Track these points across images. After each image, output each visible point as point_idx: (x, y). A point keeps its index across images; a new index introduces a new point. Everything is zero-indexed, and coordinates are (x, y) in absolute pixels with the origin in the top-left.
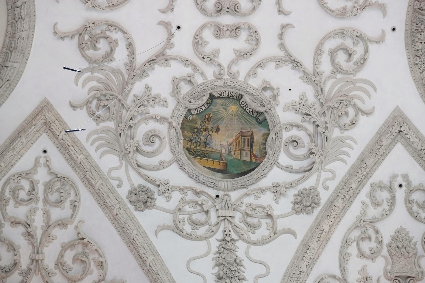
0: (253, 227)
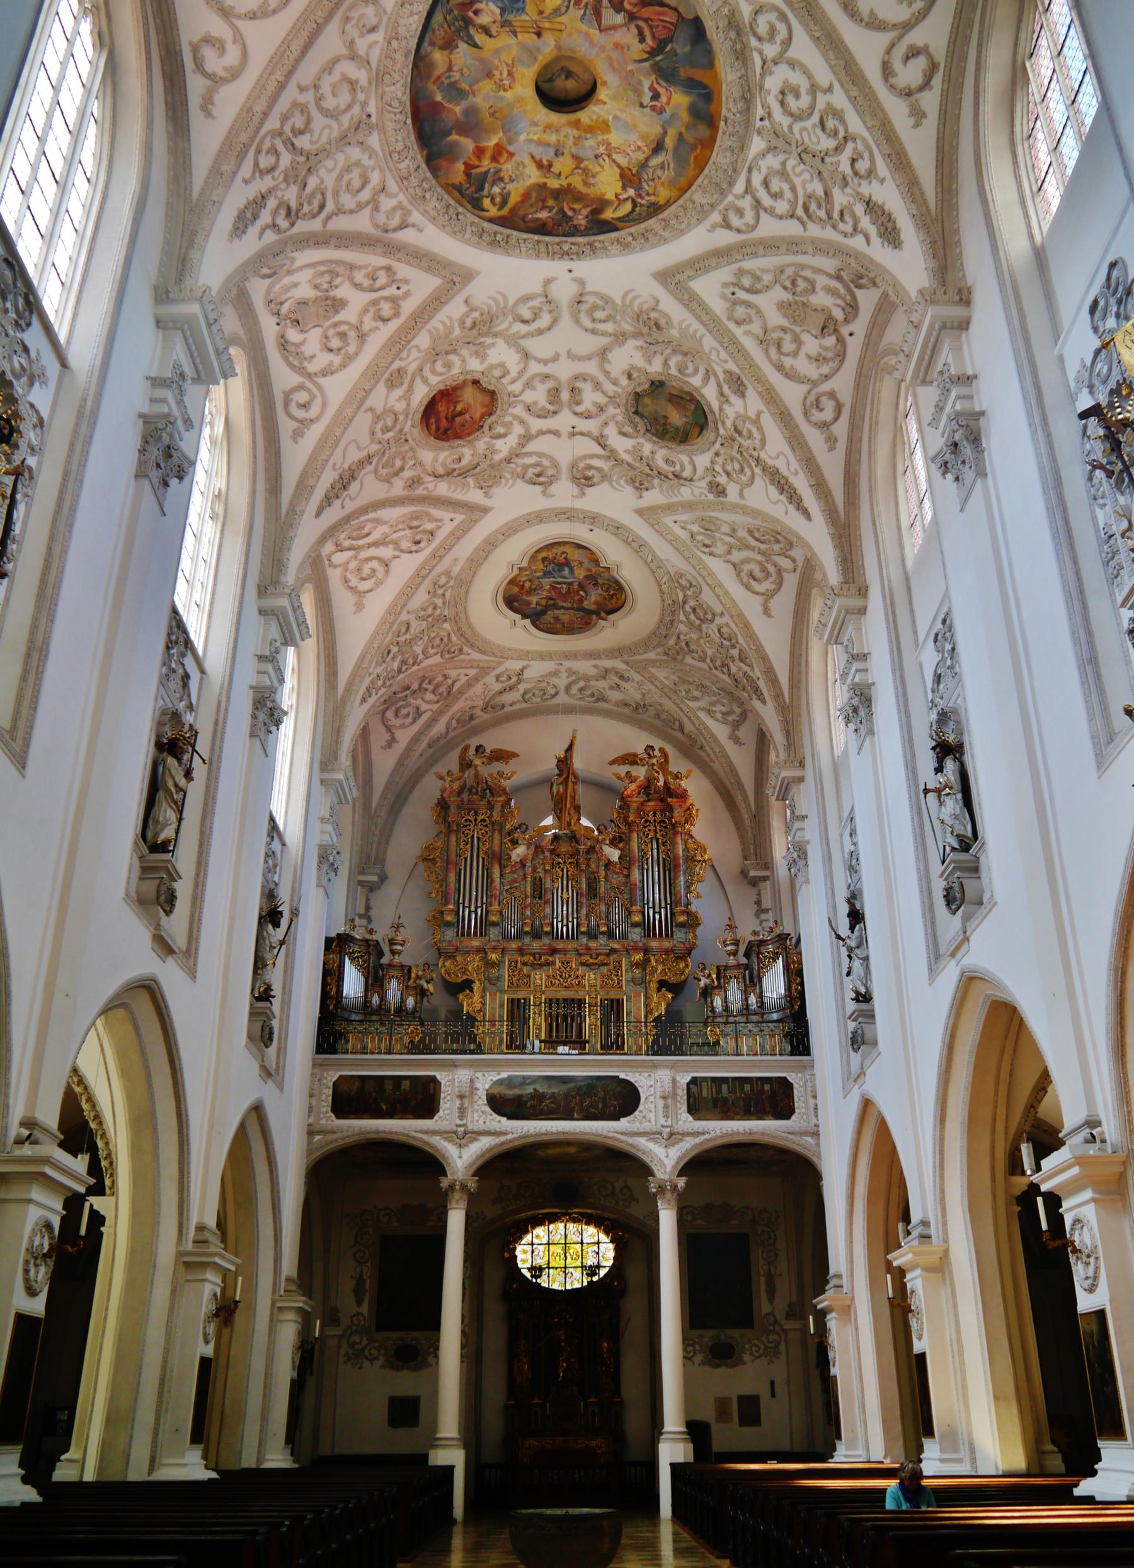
0: (750, 436)
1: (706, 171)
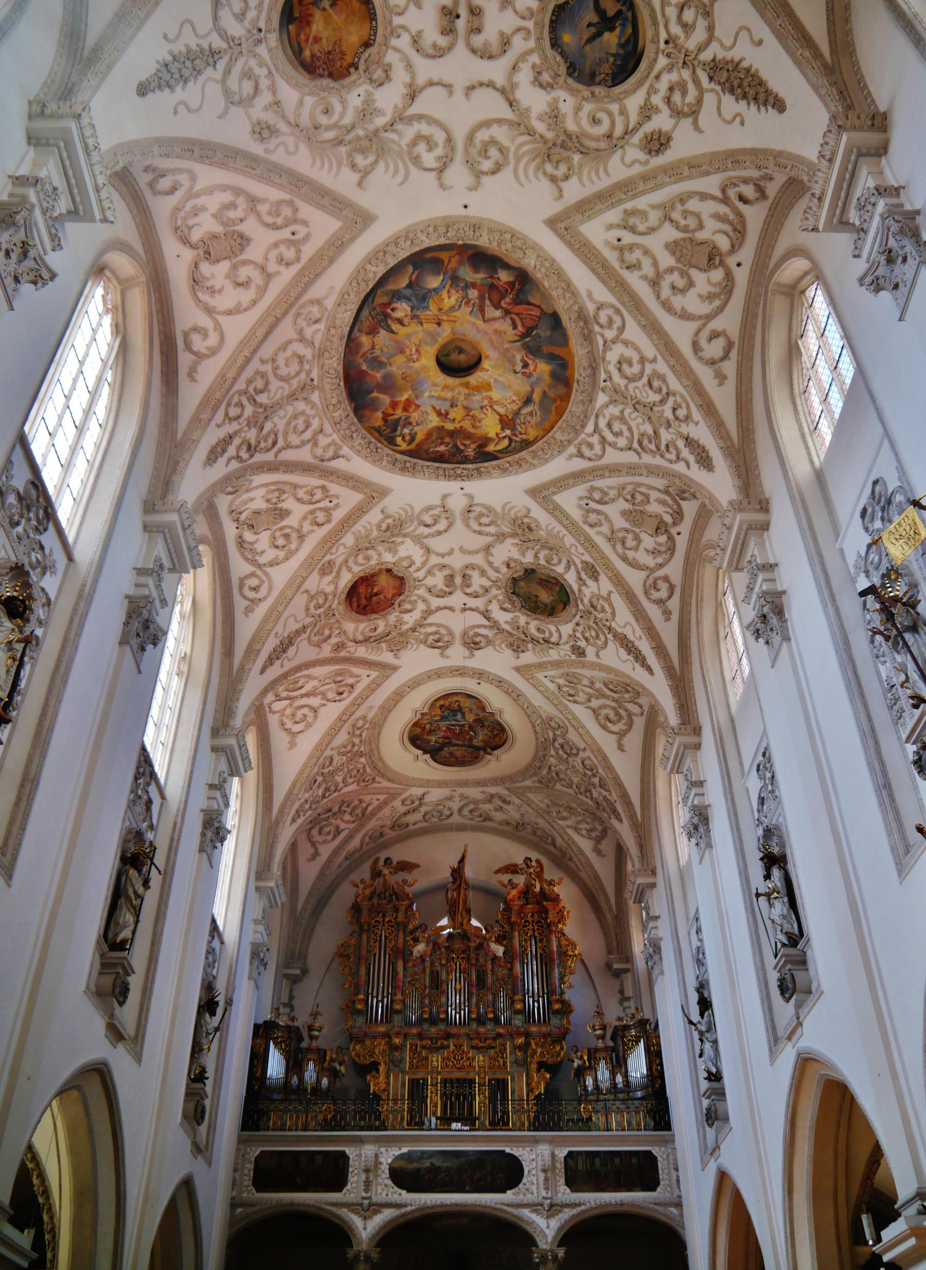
0: (603, 610)
1: (564, 417)
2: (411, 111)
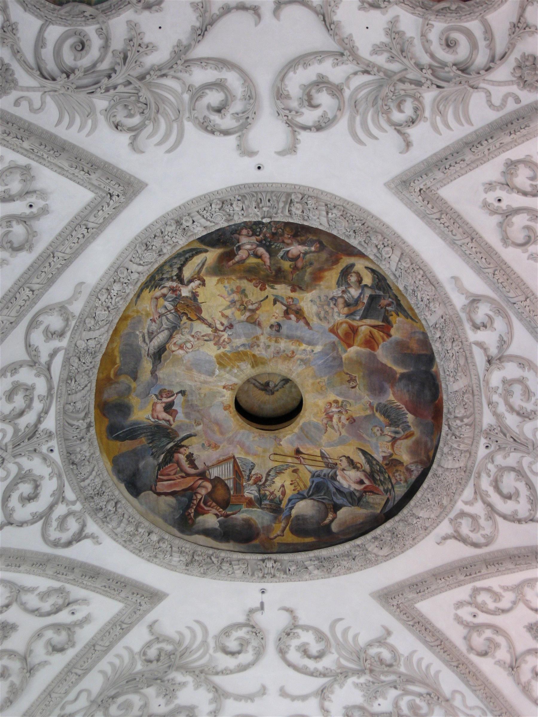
2: (321, 681)
